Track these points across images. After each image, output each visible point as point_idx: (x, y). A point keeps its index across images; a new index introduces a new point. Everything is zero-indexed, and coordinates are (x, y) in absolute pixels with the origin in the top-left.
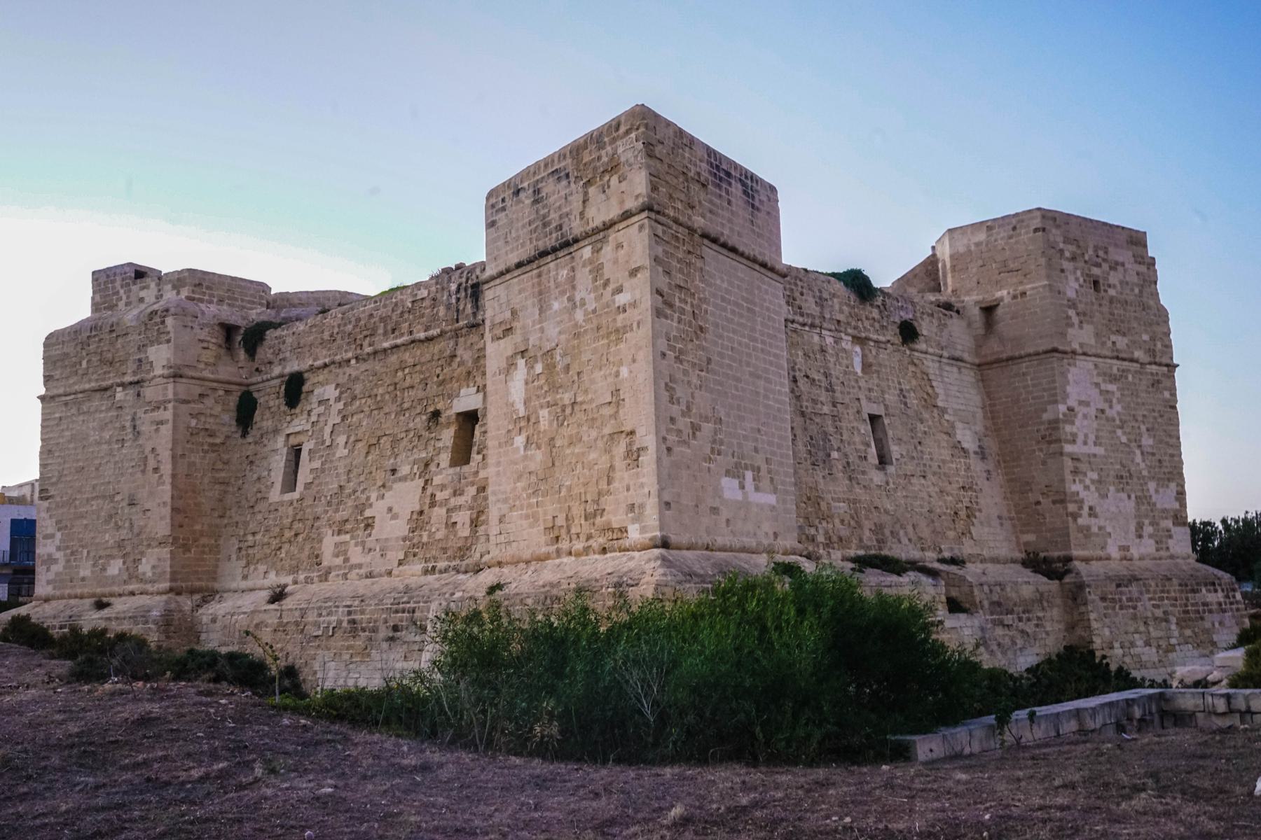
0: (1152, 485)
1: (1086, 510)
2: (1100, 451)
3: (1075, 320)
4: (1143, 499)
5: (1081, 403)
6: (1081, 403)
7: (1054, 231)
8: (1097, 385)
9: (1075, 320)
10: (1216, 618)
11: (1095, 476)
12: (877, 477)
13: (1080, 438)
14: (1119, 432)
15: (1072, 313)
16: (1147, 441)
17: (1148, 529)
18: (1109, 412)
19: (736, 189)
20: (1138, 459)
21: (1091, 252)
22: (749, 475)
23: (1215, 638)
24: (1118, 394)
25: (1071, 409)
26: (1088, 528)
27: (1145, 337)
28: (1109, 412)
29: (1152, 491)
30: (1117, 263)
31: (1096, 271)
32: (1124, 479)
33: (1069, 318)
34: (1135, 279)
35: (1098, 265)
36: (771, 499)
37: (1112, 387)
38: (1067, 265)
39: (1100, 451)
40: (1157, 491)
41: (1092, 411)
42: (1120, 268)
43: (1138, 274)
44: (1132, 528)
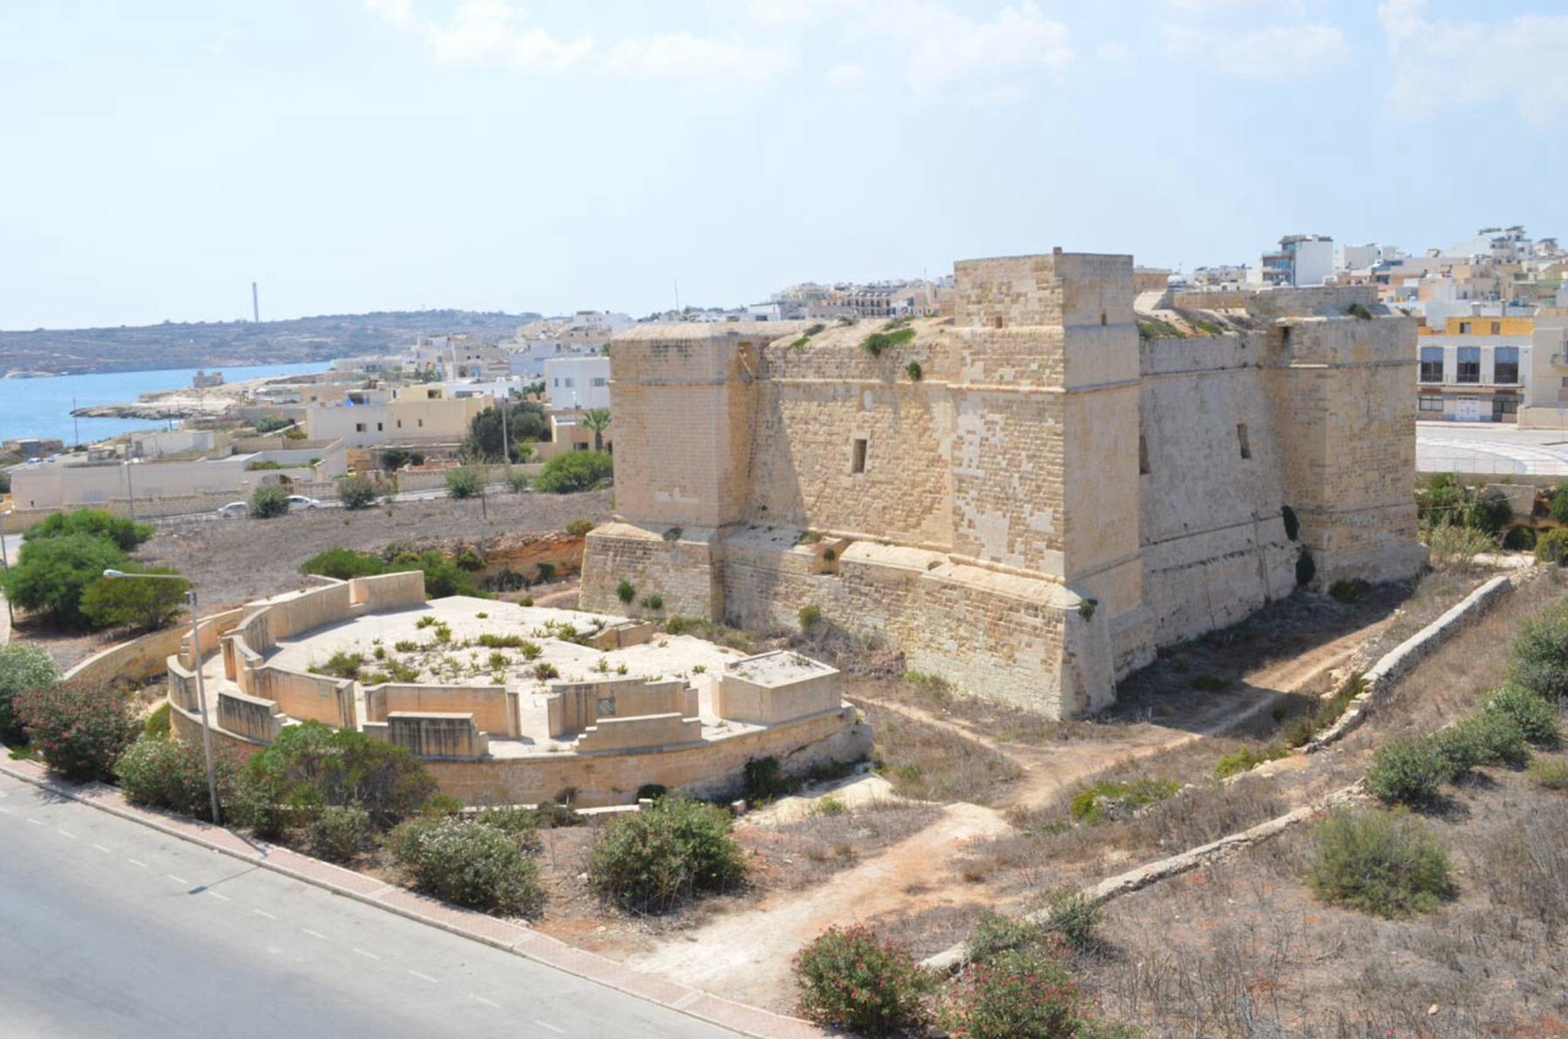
0: (1028, 507)
1: (965, 523)
2: (981, 473)
3: (969, 360)
4: (1016, 521)
5: (969, 432)
6: (969, 432)
7: (965, 280)
8: (983, 416)
9: (969, 360)
10: (1025, 638)
11: (973, 493)
12: (846, 481)
13: (965, 463)
14: (1000, 457)
15: (966, 353)
16: (1027, 466)
17: (1019, 547)
18: (993, 440)
19: (673, 352)
20: (1015, 482)
21: (995, 291)
22: (677, 490)
23: (1017, 655)
24: (1002, 423)
25: (960, 438)
26: (967, 536)
27: (1034, 366)
28: (993, 440)
29: (1027, 514)
30: (1019, 295)
31: (999, 307)
32: (1003, 500)
33: (963, 358)
34: (1036, 306)
35: (1001, 301)
36: (696, 501)
37: (996, 417)
38: (973, 308)
39: (981, 473)
40: (1032, 514)
41: (976, 439)
42: (1022, 299)
43: (1040, 300)
44: (1005, 542)
